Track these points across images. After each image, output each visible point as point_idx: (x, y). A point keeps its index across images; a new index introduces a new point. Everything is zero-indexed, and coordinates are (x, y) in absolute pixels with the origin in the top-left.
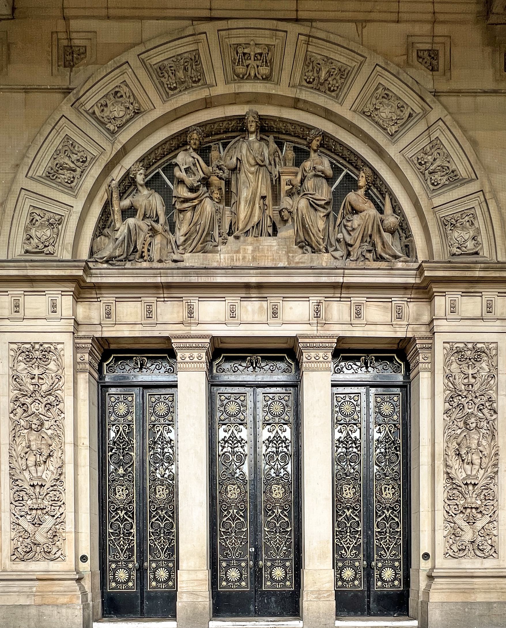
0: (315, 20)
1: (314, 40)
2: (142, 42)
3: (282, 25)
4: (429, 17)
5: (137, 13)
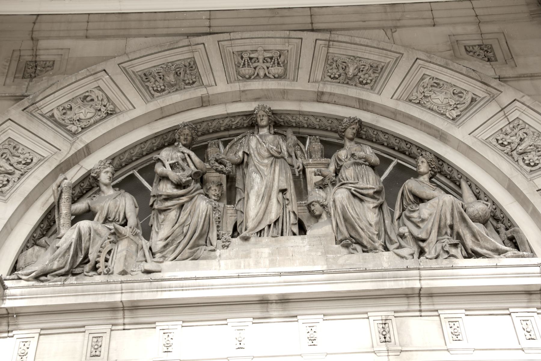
0: (335, 30)
1: (335, 43)
2: (126, 54)
3: (293, 34)
4: (473, 19)
5: (122, 32)
